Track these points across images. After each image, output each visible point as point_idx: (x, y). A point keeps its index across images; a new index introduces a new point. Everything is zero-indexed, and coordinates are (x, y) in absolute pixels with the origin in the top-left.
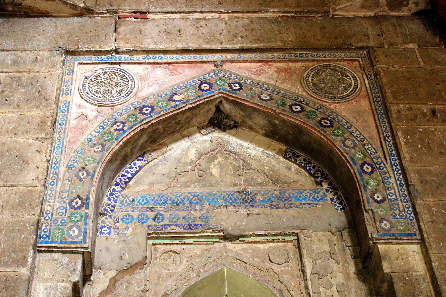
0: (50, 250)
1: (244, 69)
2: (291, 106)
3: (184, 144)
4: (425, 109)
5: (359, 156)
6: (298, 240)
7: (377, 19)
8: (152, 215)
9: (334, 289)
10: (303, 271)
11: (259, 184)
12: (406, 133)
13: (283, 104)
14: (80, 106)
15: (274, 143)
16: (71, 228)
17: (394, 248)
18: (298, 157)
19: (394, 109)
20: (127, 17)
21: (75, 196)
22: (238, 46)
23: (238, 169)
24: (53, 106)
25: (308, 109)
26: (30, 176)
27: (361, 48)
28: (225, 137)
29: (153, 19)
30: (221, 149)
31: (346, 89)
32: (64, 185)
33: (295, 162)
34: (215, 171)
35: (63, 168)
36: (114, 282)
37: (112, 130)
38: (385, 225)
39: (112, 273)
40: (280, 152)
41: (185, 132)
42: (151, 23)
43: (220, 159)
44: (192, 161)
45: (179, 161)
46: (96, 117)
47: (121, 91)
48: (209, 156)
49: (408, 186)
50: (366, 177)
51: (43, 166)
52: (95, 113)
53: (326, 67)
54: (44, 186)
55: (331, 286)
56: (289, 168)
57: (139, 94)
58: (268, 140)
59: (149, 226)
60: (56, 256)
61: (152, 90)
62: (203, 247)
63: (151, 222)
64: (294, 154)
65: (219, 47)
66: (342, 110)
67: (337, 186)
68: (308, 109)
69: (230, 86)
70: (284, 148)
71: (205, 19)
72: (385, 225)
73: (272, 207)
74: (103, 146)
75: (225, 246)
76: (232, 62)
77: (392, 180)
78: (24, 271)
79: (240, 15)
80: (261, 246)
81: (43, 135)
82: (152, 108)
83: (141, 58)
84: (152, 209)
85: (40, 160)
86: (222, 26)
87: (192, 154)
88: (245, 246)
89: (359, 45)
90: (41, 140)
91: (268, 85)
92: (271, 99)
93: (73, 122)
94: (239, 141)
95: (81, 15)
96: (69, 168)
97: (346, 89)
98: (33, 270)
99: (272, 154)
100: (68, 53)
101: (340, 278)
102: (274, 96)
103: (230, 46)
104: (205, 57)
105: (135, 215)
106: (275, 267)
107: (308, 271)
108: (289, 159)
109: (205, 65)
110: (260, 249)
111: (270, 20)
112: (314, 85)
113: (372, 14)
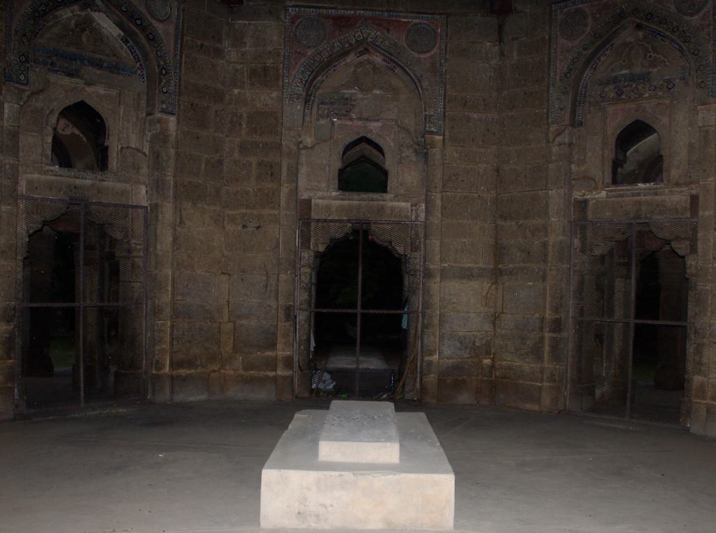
2: (136, 20)
4: (199, 42)
5: (162, 63)
9: (131, 124)
18: (128, 42)
19: (185, 38)
21: (21, 54)
25: (144, 24)
33: (126, 45)
37: (39, 9)
38: (164, 106)
43: (87, 32)
50: (162, 77)
56: (122, 48)
63: (49, 66)
64: (127, 40)
67: (144, 67)
68: (144, 24)
70: (122, 34)
73: (111, 72)
74: (35, 20)
75: (84, 88)
77: (172, 82)
105: (41, 59)
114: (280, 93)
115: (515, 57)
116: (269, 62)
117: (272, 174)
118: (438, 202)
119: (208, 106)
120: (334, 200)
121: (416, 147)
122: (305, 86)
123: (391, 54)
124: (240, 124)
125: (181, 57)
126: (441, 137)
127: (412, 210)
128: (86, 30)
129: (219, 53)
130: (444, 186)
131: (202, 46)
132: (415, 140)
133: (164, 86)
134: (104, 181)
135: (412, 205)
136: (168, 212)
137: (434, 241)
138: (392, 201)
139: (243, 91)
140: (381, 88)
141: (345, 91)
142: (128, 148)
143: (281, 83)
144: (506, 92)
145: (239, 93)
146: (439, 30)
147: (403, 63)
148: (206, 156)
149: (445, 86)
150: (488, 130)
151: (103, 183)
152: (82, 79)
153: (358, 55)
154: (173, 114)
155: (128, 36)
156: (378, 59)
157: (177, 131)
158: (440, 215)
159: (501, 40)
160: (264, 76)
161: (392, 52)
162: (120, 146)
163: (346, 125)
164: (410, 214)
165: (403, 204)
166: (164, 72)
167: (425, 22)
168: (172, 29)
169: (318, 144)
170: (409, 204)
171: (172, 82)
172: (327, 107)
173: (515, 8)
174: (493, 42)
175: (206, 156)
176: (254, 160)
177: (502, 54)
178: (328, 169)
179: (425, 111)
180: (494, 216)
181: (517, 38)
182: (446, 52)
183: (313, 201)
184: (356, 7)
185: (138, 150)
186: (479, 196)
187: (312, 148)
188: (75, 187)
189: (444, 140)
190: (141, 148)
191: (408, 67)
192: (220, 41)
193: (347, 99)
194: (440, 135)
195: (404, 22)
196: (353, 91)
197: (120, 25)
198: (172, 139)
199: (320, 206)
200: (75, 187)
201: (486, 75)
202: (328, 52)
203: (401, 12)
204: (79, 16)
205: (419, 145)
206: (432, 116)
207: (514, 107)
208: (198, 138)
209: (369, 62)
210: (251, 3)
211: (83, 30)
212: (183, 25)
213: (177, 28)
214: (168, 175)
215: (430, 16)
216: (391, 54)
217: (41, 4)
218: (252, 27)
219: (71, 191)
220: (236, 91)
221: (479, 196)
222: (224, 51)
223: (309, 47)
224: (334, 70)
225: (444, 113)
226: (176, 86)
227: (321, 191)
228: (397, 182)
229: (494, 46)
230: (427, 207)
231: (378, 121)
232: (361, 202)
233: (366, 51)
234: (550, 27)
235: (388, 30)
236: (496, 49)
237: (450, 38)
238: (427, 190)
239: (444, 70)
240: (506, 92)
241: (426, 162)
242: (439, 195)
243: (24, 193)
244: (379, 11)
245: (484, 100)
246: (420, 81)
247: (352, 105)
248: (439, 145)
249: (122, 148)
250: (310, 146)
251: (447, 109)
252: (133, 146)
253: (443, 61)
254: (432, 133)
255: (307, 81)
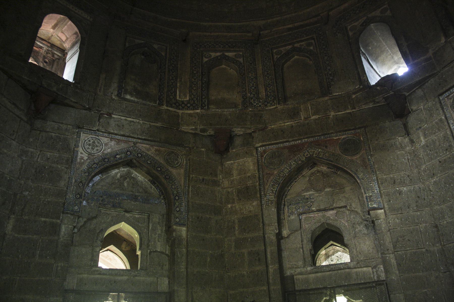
0: (67, 213)
1: (143, 147)
3: (117, 171)
4: (201, 178)
5: (175, 192)
6: (149, 216)
7: (195, 135)
8: (101, 199)
10: (148, 227)
11: (140, 192)
12: (192, 187)
13: (155, 166)
14: (82, 153)
15: (148, 176)
16: (75, 206)
17: (178, 228)
19: (191, 176)
20: (104, 114)
22: (143, 138)
23: (133, 184)
24: (72, 153)
25: (163, 170)
26: (62, 183)
27: (187, 147)
28: (132, 170)
29: (114, 118)
30: (129, 173)
31: (177, 164)
32: (74, 188)
34: (126, 184)
35: (74, 181)
36: (85, 222)
38: (178, 220)
39: (85, 219)
40: (149, 180)
41: (117, 166)
42: (112, 119)
44: (118, 179)
45: (113, 177)
46: (87, 160)
47: (97, 150)
48: (124, 177)
49: (188, 207)
50: (176, 201)
51: (67, 180)
52: (87, 158)
53: (173, 152)
54: (67, 188)
55: (156, 234)
56: (151, 187)
57: (104, 152)
58: (146, 174)
59: (100, 204)
60: (69, 215)
61: (109, 150)
62: (117, 213)
63: (100, 202)
64: (154, 182)
65: (136, 136)
66: (174, 171)
69: (138, 155)
70: (151, 179)
71: (133, 121)
72: (178, 220)
74: (89, 173)
76: (140, 143)
77: (184, 204)
78: (59, 221)
79: (147, 122)
80: (136, 216)
81: (67, 166)
82: (108, 159)
83: (106, 135)
84: (102, 197)
85: (66, 176)
86: (139, 127)
87: (119, 175)
88: (131, 215)
89: (186, 146)
90: (67, 168)
91: (151, 156)
92: (151, 163)
93: (78, 160)
94: (136, 173)
95: (86, 110)
96: (76, 181)
97: (177, 164)
98: (61, 221)
99: (146, 180)
100: (79, 127)
101: (160, 232)
102: (152, 161)
103: (140, 137)
104: (130, 139)
105: (96, 198)
106: (140, 224)
107: (150, 228)
108: (152, 184)
109: (130, 143)
110: (135, 217)
111: (157, 127)
112: (167, 160)
113: (194, 132)
114: (259, 201)
115: (423, 140)
116: (249, 183)
117: (259, 259)
118: (393, 261)
119: (210, 218)
120: (310, 273)
121: (365, 222)
122: (275, 194)
123: (332, 161)
124: (234, 228)
125: (189, 187)
126: (383, 210)
127: (373, 273)
128: (127, 179)
129: (216, 183)
130: (395, 247)
131: (203, 179)
132: (364, 218)
133: (178, 207)
134: (136, 276)
135: (372, 268)
136: (181, 294)
137: (398, 295)
138: (355, 268)
139: (234, 205)
140: (330, 187)
141: (305, 194)
142: (156, 251)
143: (258, 195)
144: (424, 167)
145: (231, 207)
146: (362, 138)
147: (341, 165)
148: (210, 252)
149: (376, 173)
150: (418, 197)
151: (137, 278)
152: (122, 208)
153: (310, 168)
154: (184, 225)
155: (155, 180)
156: (324, 168)
157: (187, 235)
158: (398, 272)
159: (408, 134)
160: (246, 193)
161: (332, 159)
162: (149, 251)
163: (311, 217)
164: (372, 276)
165: (365, 269)
166: (177, 198)
167: (350, 136)
168: (182, 171)
169: (292, 233)
170: (370, 269)
171: (184, 204)
172: (294, 207)
173: (412, 110)
174: (403, 136)
175: (210, 252)
176: (245, 251)
177: (412, 142)
178: (302, 251)
179: (365, 193)
180: (446, 265)
181: (420, 128)
182: (370, 150)
183: (295, 277)
184: (302, 137)
185: (162, 253)
186: (427, 250)
187: (288, 237)
188: (115, 282)
189: (385, 211)
190: (164, 251)
191: (345, 167)
192: (216, 176)
193: (307, 199)
194: (381, 209)
195: (336, 139)
196: (311, 193)
197: (149, 173)
198: (184, 242)
199: (300, 279)
200: (115, 282)
201: (405, 159)
202: (288, 169)
203: (332, 133)
204: (124, 171)
205: (367, 221)
206: (371, 196)
207: (434, 174)
208: (203, 240)
209: (318, 171)
210: (234, 150)
211: (126, 179)
212: (190, 168)
213: (185, 171)
214: (182, 268)
215: (353, 131)
216: (332, 161)
217: (94, 164)
218: (236, 164)
219: (111, 284)
220: (229, 206)
221: (427, 250)
222: (219, 182)
223: (275, 169)
224: (295, 182)
225: (380, 191)
226: (186, 206)
227: (299, 268)
228: (357, 252)
229: (405, 138)
230: (384, 268)
231: (333, 209)
232: (331, 272)
233: (314, 164)
234: (443, 111)
235: (326, 147)
236: (407, 140)
237: (371, 141)
238: (381, 254)
239: (372, 163)
240: (424, 167)
241: (376, 233)
242: (392, 256)
243: (75, 288)
244: (317, 136)
245: (408, 176)
246: (355, 174)
247: (312, 202)
248: (383, 216)
249: (150, 252)
250: (286, 236)
251: (382, 189)
252: (159, 250)
253: (370, 157)
254: (374, 209)
255: (276, 190)
